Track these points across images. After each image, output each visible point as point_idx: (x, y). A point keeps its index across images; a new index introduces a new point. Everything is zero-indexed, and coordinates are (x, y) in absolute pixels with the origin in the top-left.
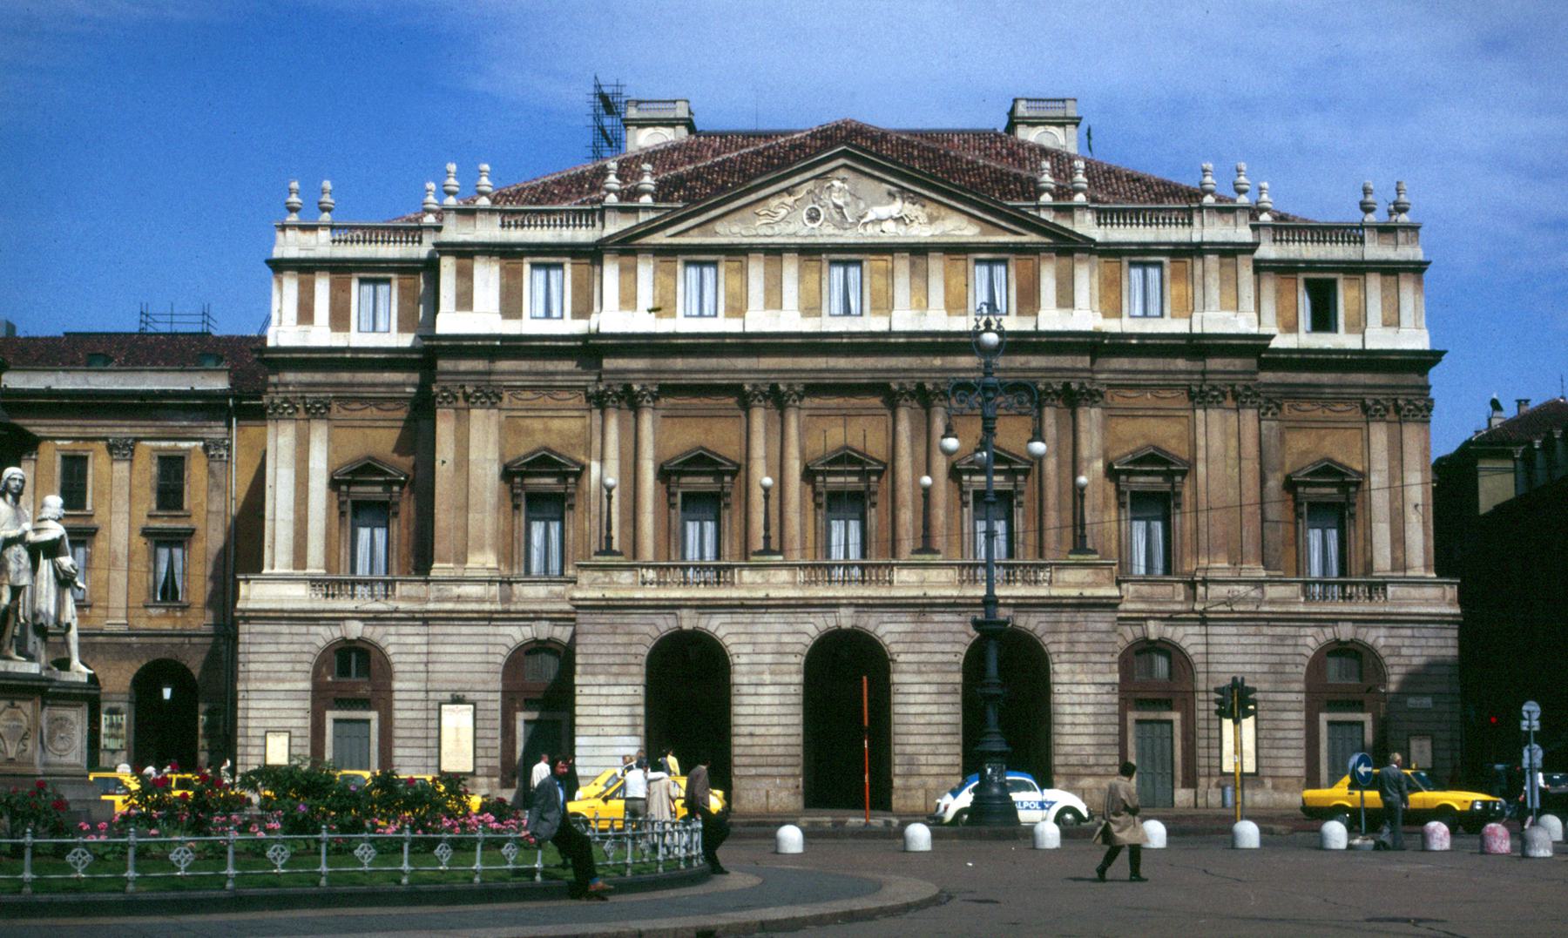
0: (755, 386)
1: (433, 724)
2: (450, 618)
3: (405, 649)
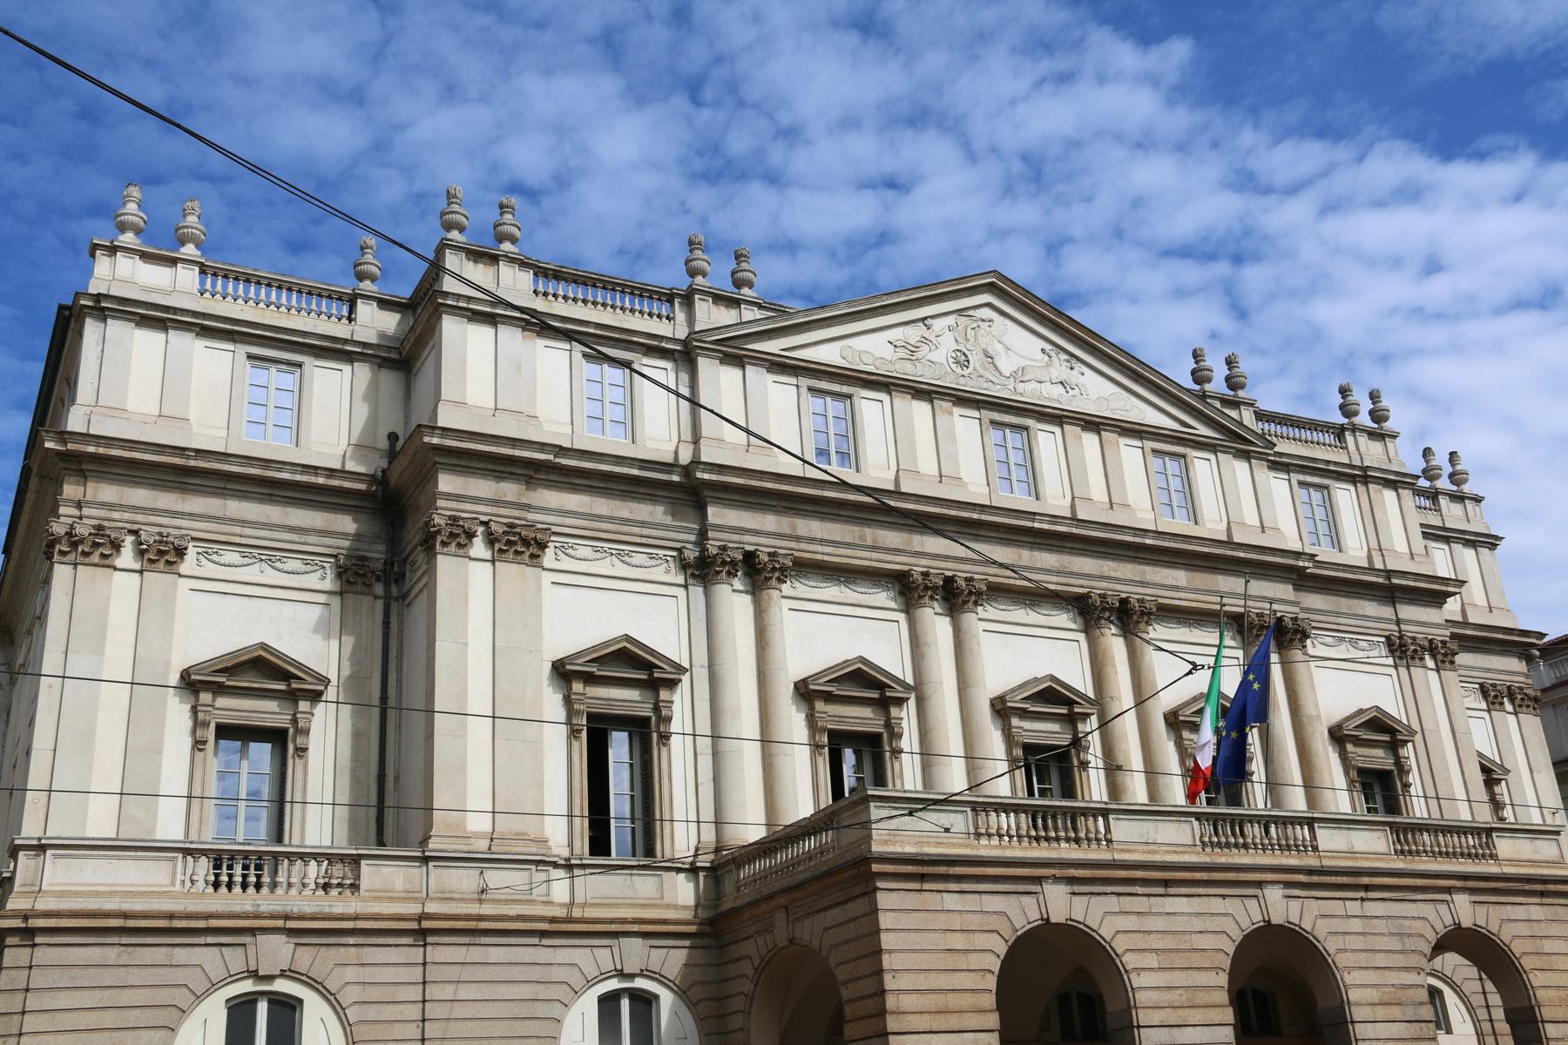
0: (925, 575)
2: (473, 931)
3: (374, 994)
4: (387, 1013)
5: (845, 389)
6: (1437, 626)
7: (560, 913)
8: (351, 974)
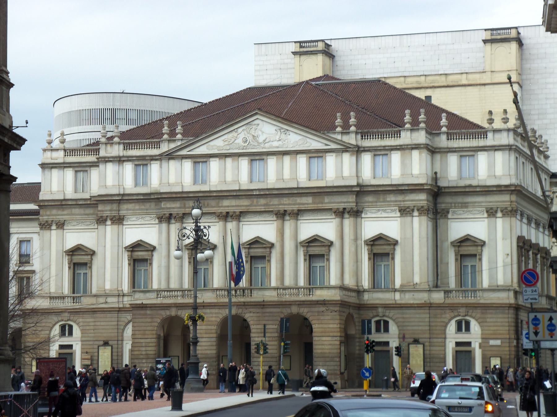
1: (96, 354)
3: (85, 324)
4: (88, 328)
5: (205, 160)
6: (421, 200)
7: (121, 306)
8: (81, 320)
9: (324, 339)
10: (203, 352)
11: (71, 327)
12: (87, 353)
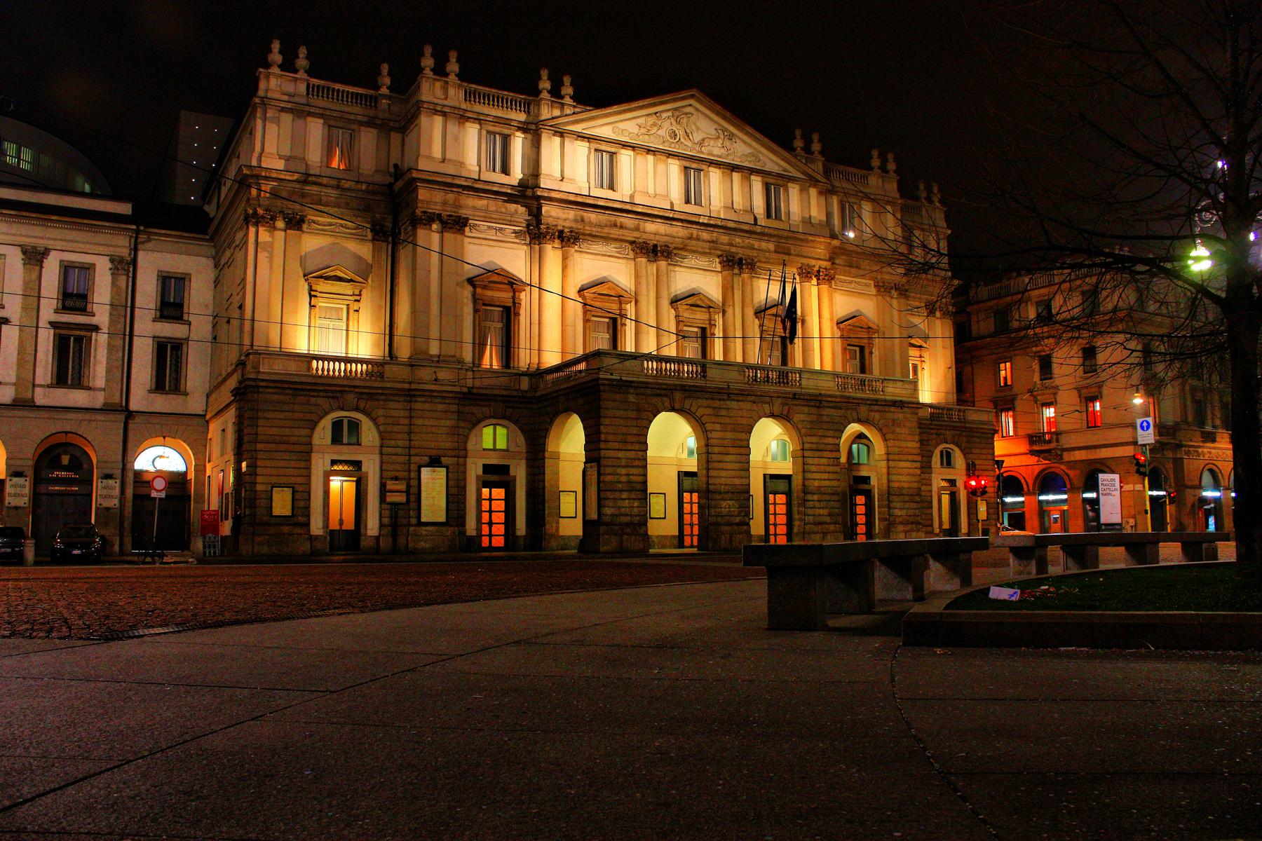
2: (430, 395)
3: (390, 421)
8: (381, 412)
9: (902, 464)
10: (729, 481)
11: (355, 426)
12: (396, 479)
